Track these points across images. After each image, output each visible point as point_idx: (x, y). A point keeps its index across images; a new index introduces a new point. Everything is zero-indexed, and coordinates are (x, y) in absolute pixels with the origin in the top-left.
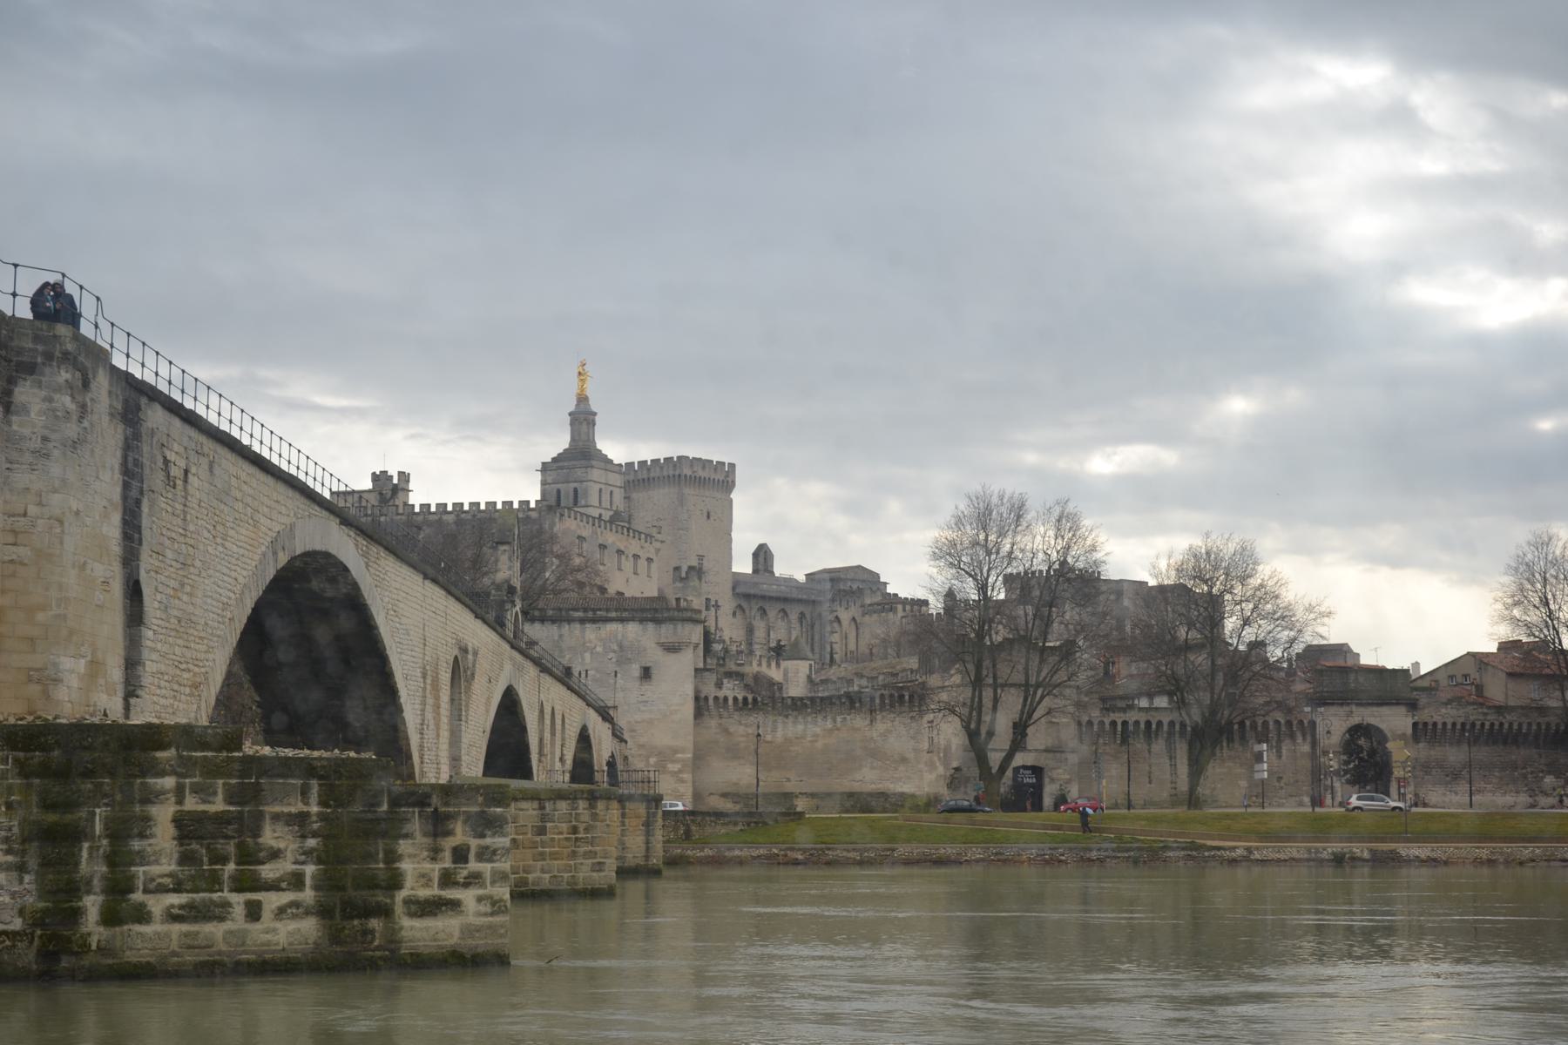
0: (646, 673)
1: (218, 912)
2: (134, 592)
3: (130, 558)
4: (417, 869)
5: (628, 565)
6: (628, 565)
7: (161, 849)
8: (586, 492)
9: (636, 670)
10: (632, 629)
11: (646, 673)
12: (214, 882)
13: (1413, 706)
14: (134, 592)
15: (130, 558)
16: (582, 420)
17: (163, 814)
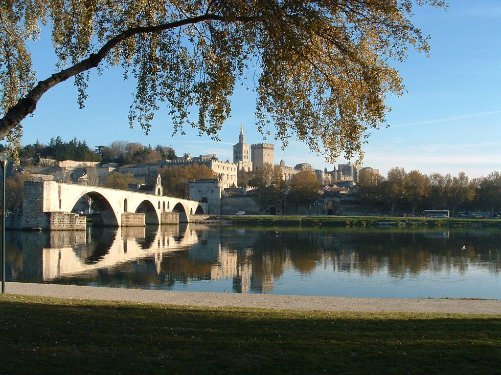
0: (212, 191)
1: (60, 226)
2: (60, 201)
3: (59, 197)
4: (78, 222)
5: (230, 169)
6: (230, 169)
7: (56, 221)
8: (242, 151)
9: (211, 191)
10: (210, 184)
11: (212, 191)
12: (60, 223)
13: (340, 197)
14: (60, 201)
15: (59, 197)
16: (241, 137)
17: (56, 218)
